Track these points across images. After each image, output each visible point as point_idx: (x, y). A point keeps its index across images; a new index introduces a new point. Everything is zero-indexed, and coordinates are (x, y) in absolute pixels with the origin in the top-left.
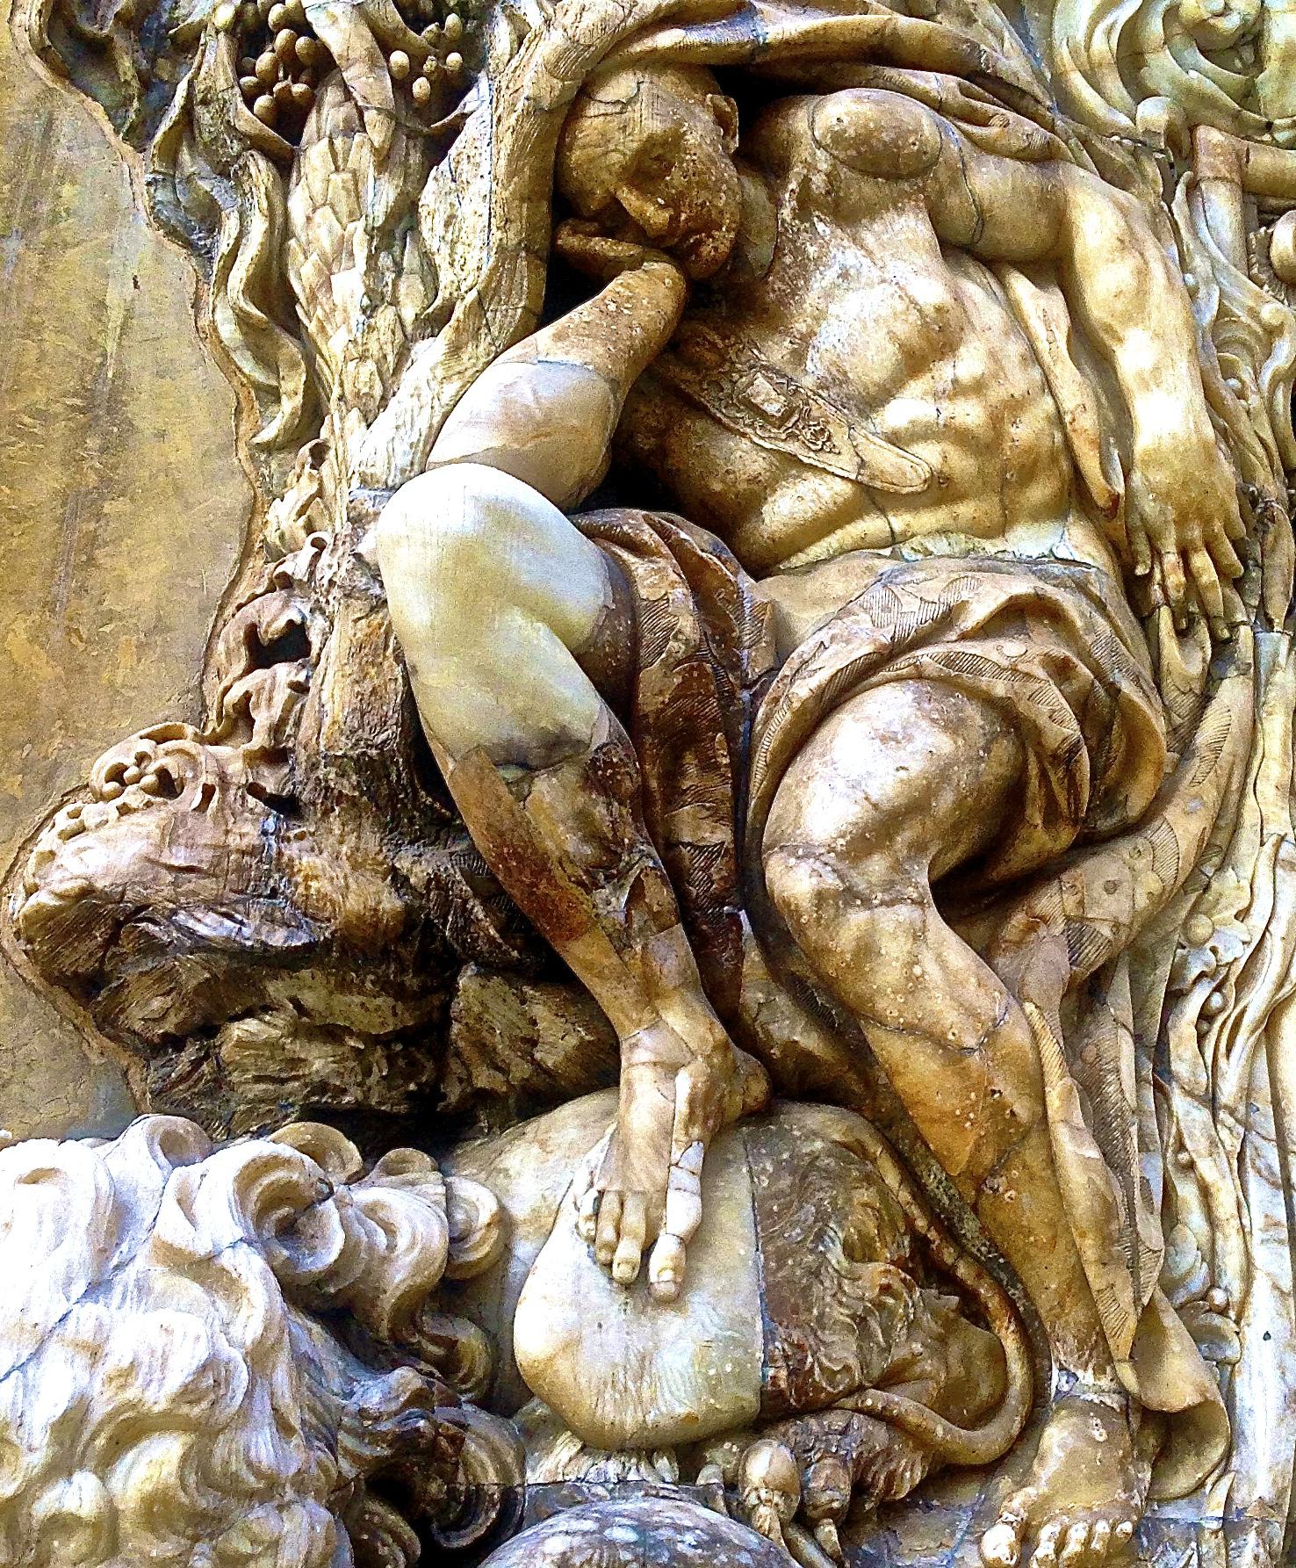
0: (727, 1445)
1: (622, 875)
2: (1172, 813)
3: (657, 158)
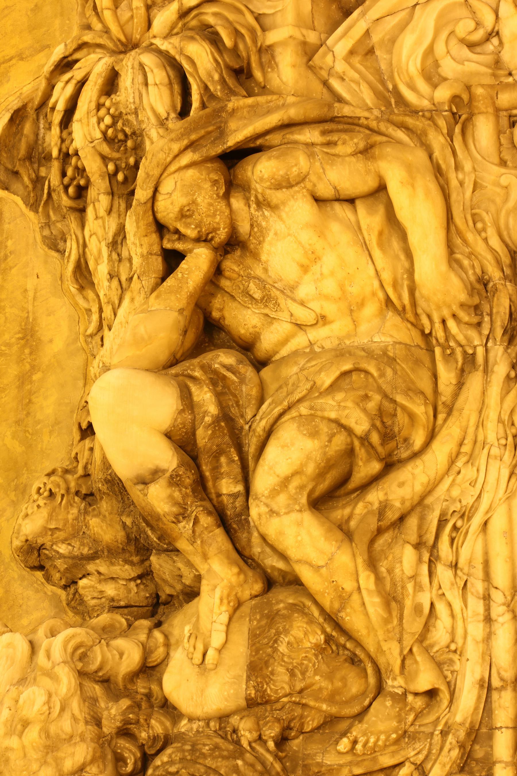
0: (236, 717)
1: (189, 516)
2: (436, 445)
3: (188, 210)
